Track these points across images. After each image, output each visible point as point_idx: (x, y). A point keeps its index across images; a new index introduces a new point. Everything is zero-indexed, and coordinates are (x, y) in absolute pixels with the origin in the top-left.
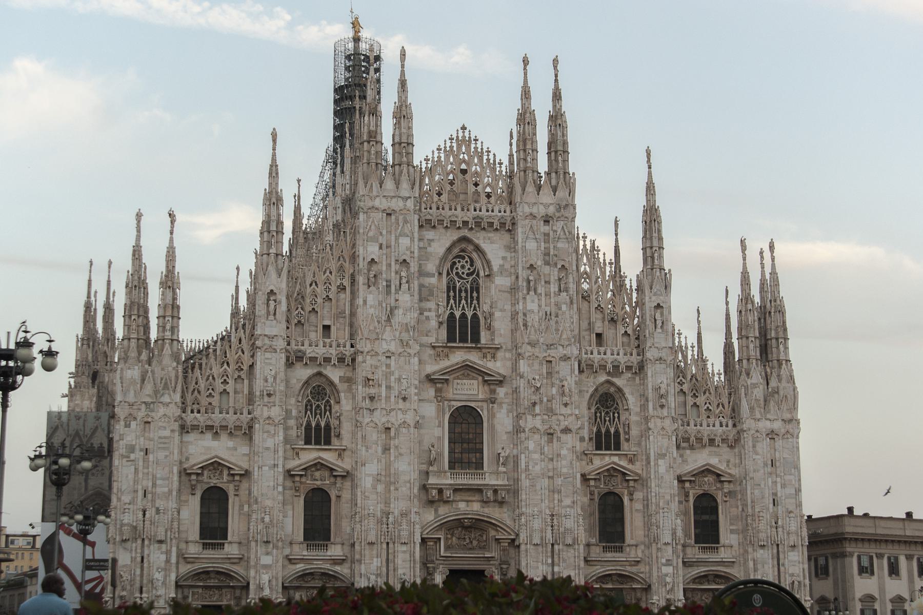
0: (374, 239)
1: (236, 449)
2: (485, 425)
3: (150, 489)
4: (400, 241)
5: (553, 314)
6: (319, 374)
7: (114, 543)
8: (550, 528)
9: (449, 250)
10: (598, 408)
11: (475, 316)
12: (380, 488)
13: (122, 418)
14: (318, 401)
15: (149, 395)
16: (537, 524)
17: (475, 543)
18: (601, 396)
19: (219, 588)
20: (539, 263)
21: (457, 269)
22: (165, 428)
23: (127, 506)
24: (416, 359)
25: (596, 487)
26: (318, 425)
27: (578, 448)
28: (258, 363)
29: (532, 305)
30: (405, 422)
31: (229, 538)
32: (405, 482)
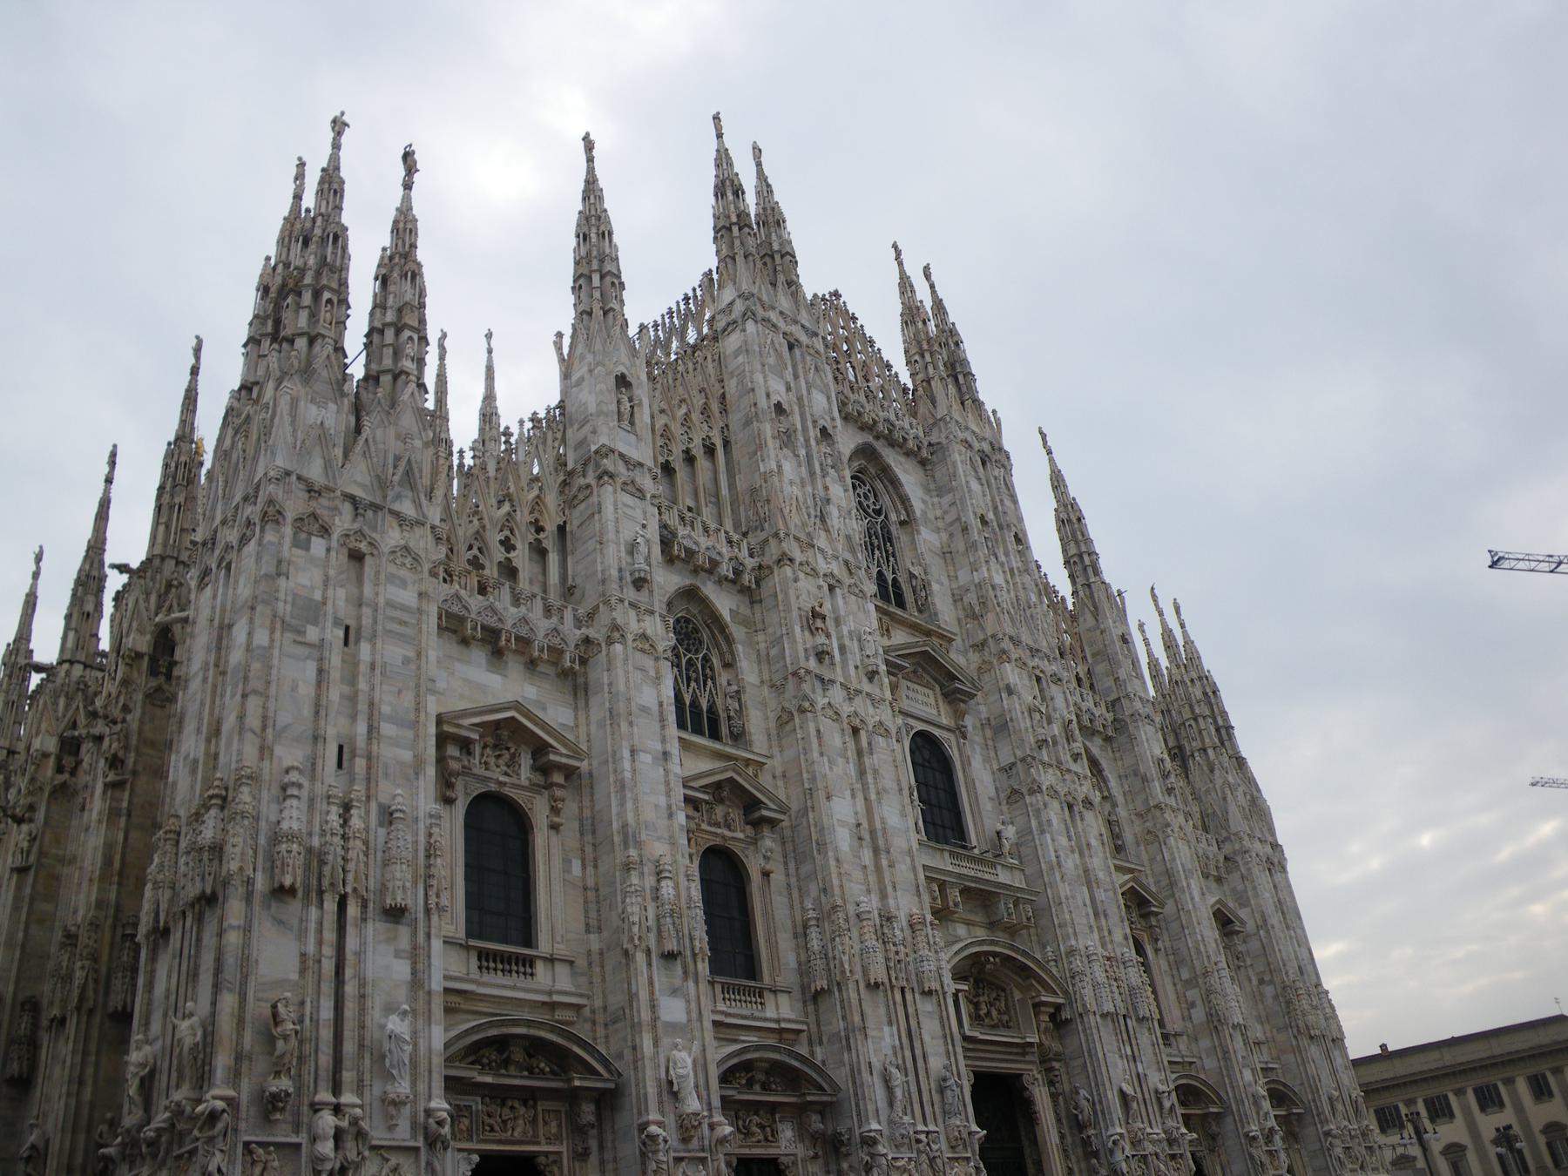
1: (544, 709)
3: (361, 742)
7: (248, 898)
12: (867, 856)
13: (290, 515)
14: (688, 651)
15: (360, 485)
16: (1100, 976)
17: (994, 1013)
19: (529, 1097)
20: (991, 516)
22: (403, 584)
23: (294, 777)
26: (695, 703)
28: (608, 508)
30: (881, 723)
31: (544, 946)
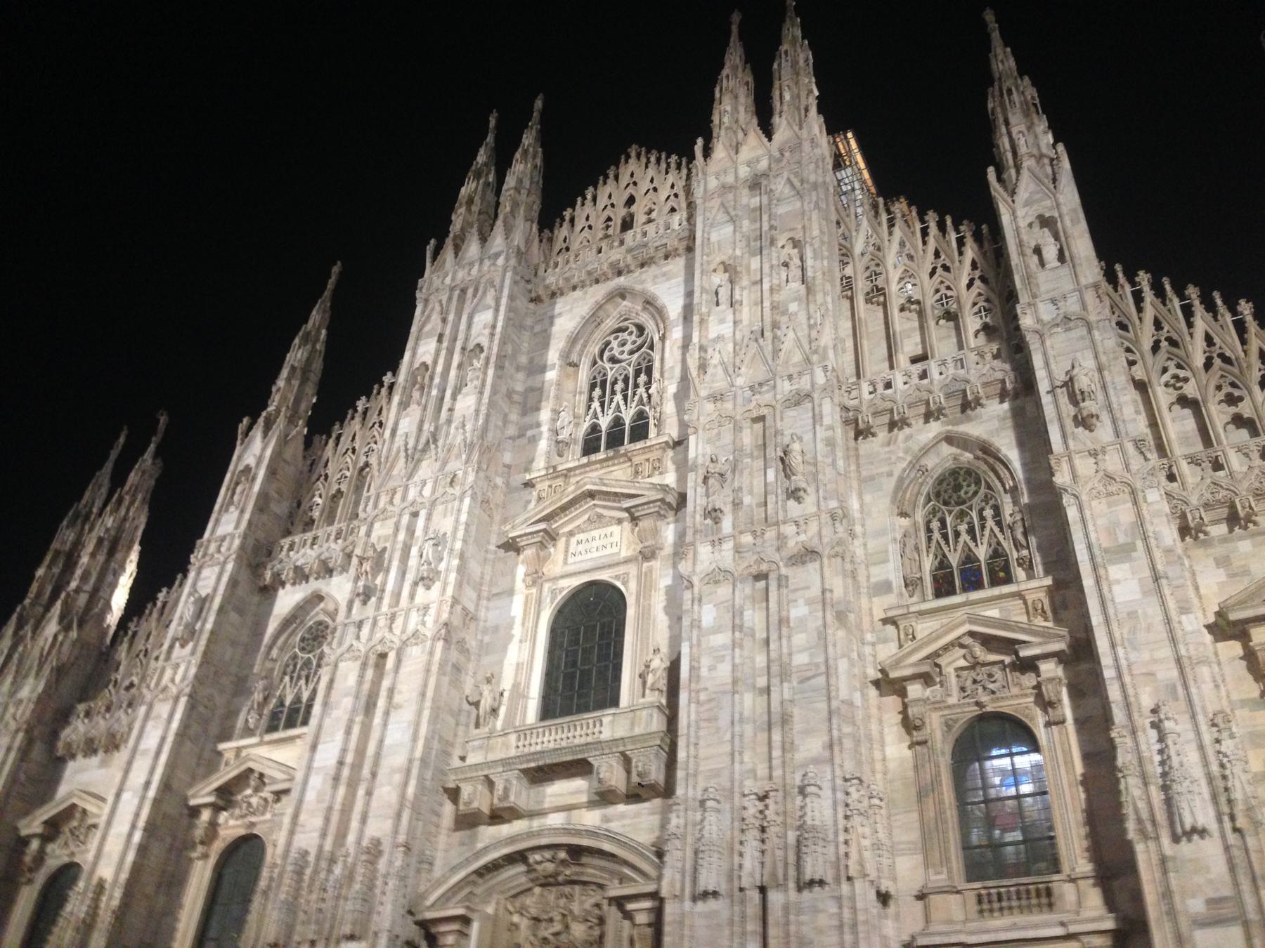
0: (429, 335)
2: (631, 612)
4: (476, 319)
5: (768, 328)
6: (318, 598)
8: (752, 836)
9: (594, 319)
10: (934, 512)
11: (641, 415)
14: (310, 652)
16: (716, 825)
18: (940, 481)
21: (612, 349)
24: (467, 501)
25: (938, 705)
27: (838, 593)
29: (719, 326)
32: (394, 771)
